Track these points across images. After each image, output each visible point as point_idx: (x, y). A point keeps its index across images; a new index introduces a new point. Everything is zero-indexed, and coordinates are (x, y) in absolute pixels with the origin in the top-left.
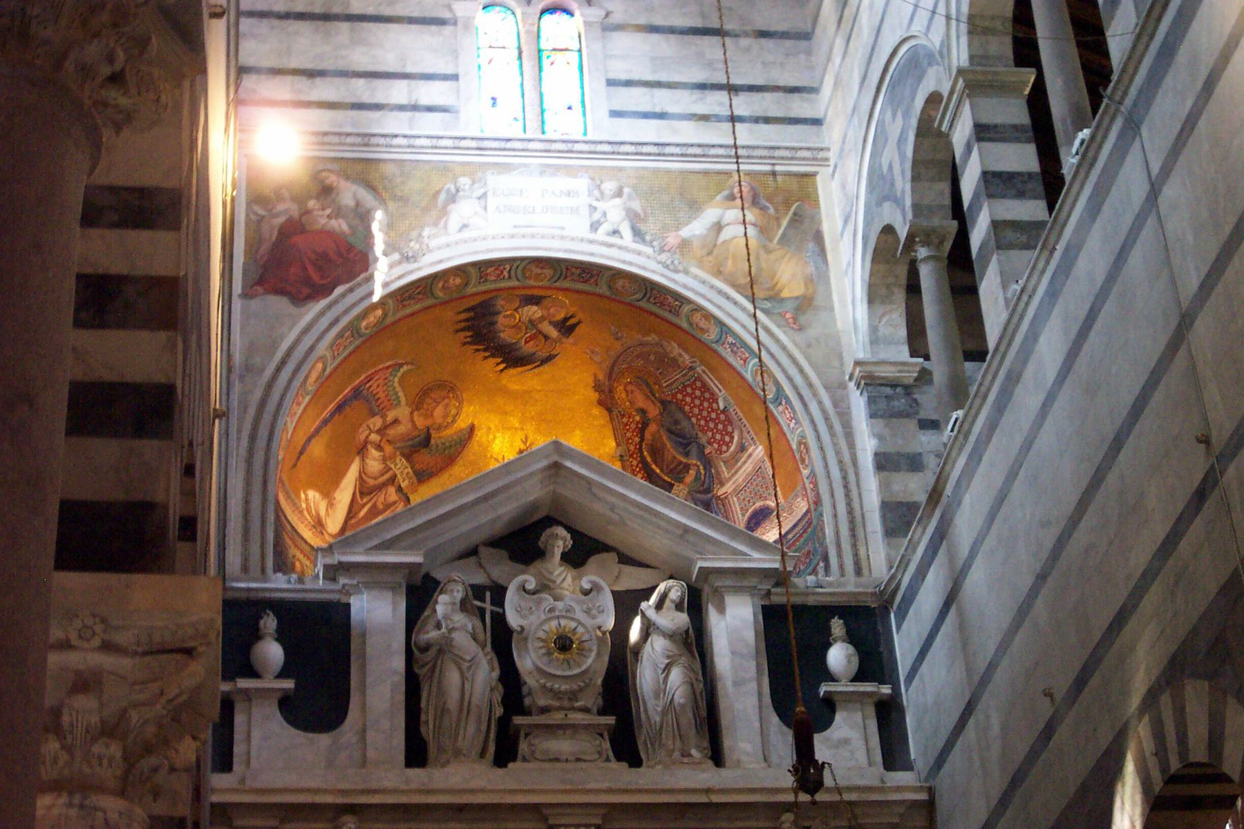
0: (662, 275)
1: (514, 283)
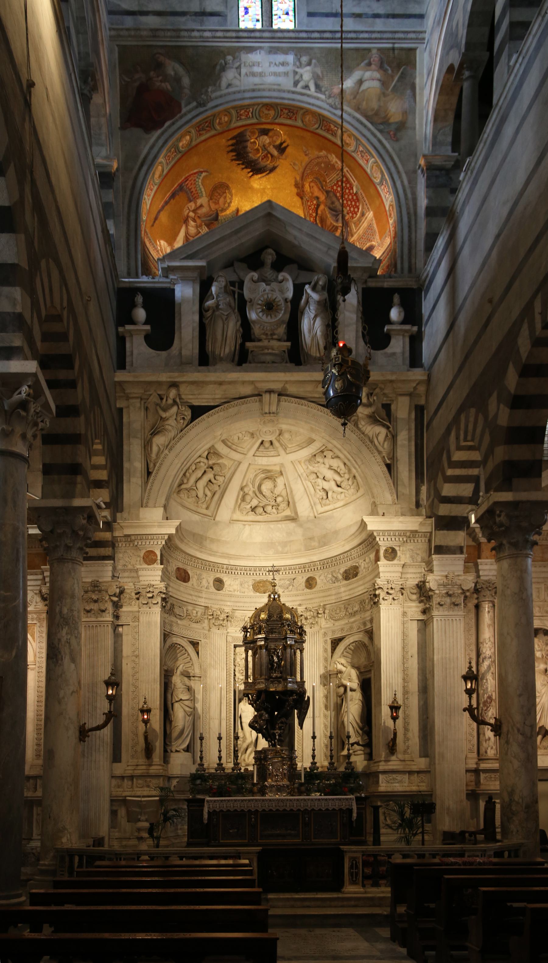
0: (329, 111)
1: (254, 121)
